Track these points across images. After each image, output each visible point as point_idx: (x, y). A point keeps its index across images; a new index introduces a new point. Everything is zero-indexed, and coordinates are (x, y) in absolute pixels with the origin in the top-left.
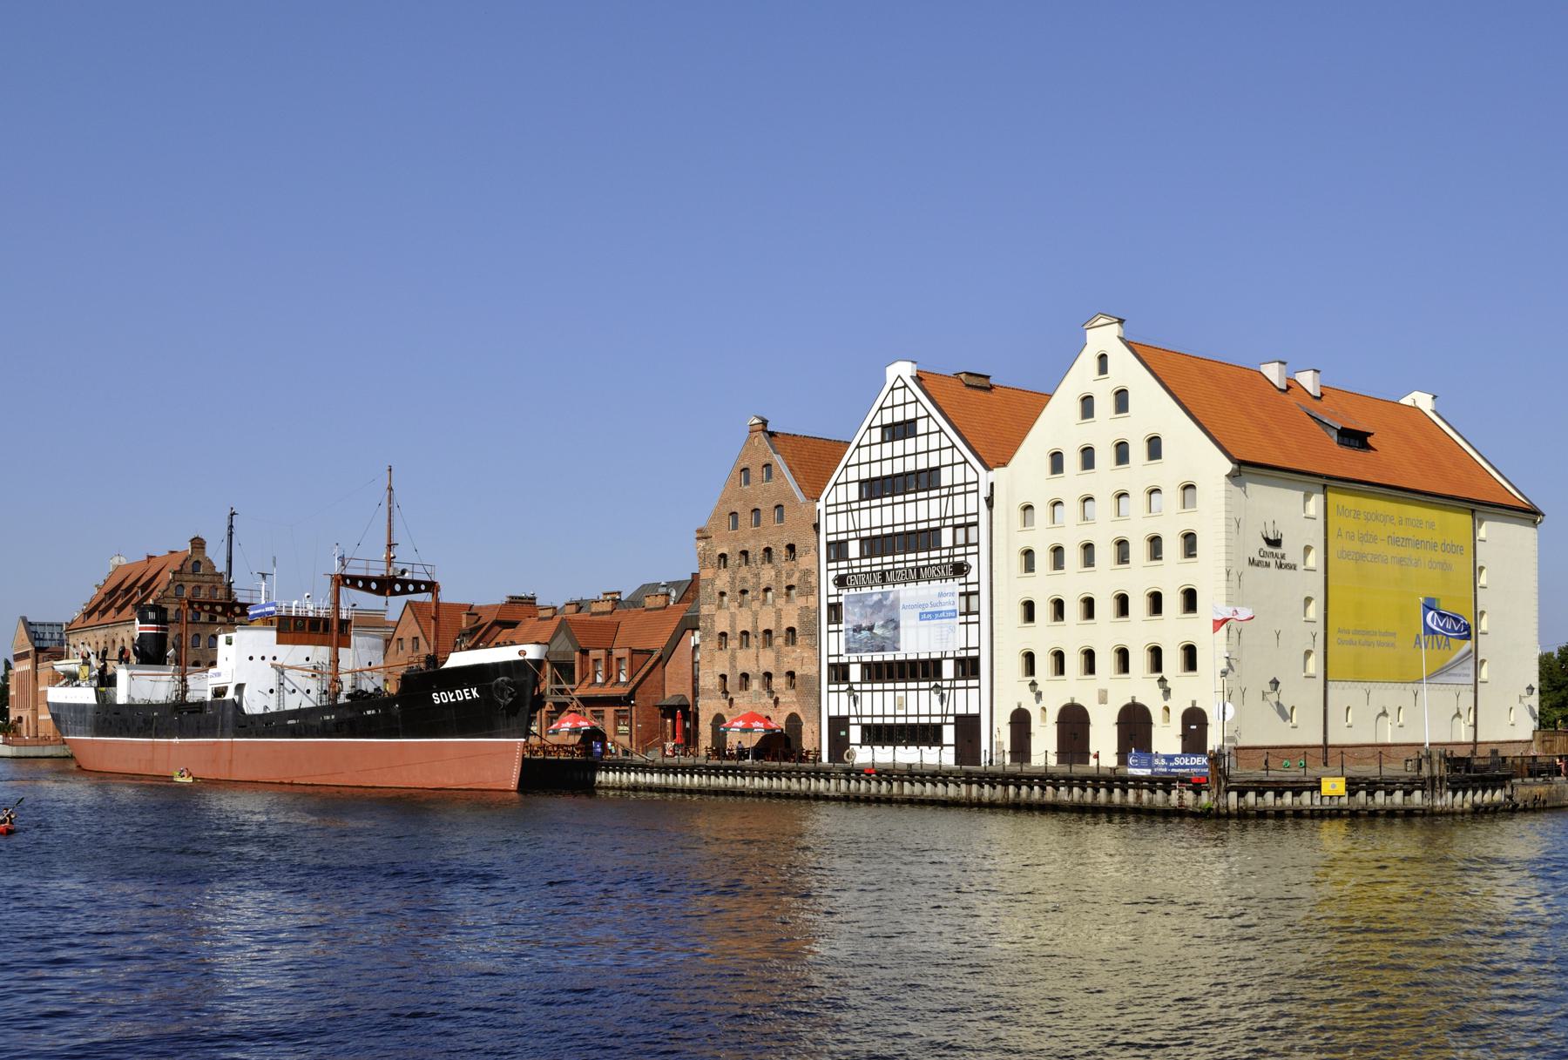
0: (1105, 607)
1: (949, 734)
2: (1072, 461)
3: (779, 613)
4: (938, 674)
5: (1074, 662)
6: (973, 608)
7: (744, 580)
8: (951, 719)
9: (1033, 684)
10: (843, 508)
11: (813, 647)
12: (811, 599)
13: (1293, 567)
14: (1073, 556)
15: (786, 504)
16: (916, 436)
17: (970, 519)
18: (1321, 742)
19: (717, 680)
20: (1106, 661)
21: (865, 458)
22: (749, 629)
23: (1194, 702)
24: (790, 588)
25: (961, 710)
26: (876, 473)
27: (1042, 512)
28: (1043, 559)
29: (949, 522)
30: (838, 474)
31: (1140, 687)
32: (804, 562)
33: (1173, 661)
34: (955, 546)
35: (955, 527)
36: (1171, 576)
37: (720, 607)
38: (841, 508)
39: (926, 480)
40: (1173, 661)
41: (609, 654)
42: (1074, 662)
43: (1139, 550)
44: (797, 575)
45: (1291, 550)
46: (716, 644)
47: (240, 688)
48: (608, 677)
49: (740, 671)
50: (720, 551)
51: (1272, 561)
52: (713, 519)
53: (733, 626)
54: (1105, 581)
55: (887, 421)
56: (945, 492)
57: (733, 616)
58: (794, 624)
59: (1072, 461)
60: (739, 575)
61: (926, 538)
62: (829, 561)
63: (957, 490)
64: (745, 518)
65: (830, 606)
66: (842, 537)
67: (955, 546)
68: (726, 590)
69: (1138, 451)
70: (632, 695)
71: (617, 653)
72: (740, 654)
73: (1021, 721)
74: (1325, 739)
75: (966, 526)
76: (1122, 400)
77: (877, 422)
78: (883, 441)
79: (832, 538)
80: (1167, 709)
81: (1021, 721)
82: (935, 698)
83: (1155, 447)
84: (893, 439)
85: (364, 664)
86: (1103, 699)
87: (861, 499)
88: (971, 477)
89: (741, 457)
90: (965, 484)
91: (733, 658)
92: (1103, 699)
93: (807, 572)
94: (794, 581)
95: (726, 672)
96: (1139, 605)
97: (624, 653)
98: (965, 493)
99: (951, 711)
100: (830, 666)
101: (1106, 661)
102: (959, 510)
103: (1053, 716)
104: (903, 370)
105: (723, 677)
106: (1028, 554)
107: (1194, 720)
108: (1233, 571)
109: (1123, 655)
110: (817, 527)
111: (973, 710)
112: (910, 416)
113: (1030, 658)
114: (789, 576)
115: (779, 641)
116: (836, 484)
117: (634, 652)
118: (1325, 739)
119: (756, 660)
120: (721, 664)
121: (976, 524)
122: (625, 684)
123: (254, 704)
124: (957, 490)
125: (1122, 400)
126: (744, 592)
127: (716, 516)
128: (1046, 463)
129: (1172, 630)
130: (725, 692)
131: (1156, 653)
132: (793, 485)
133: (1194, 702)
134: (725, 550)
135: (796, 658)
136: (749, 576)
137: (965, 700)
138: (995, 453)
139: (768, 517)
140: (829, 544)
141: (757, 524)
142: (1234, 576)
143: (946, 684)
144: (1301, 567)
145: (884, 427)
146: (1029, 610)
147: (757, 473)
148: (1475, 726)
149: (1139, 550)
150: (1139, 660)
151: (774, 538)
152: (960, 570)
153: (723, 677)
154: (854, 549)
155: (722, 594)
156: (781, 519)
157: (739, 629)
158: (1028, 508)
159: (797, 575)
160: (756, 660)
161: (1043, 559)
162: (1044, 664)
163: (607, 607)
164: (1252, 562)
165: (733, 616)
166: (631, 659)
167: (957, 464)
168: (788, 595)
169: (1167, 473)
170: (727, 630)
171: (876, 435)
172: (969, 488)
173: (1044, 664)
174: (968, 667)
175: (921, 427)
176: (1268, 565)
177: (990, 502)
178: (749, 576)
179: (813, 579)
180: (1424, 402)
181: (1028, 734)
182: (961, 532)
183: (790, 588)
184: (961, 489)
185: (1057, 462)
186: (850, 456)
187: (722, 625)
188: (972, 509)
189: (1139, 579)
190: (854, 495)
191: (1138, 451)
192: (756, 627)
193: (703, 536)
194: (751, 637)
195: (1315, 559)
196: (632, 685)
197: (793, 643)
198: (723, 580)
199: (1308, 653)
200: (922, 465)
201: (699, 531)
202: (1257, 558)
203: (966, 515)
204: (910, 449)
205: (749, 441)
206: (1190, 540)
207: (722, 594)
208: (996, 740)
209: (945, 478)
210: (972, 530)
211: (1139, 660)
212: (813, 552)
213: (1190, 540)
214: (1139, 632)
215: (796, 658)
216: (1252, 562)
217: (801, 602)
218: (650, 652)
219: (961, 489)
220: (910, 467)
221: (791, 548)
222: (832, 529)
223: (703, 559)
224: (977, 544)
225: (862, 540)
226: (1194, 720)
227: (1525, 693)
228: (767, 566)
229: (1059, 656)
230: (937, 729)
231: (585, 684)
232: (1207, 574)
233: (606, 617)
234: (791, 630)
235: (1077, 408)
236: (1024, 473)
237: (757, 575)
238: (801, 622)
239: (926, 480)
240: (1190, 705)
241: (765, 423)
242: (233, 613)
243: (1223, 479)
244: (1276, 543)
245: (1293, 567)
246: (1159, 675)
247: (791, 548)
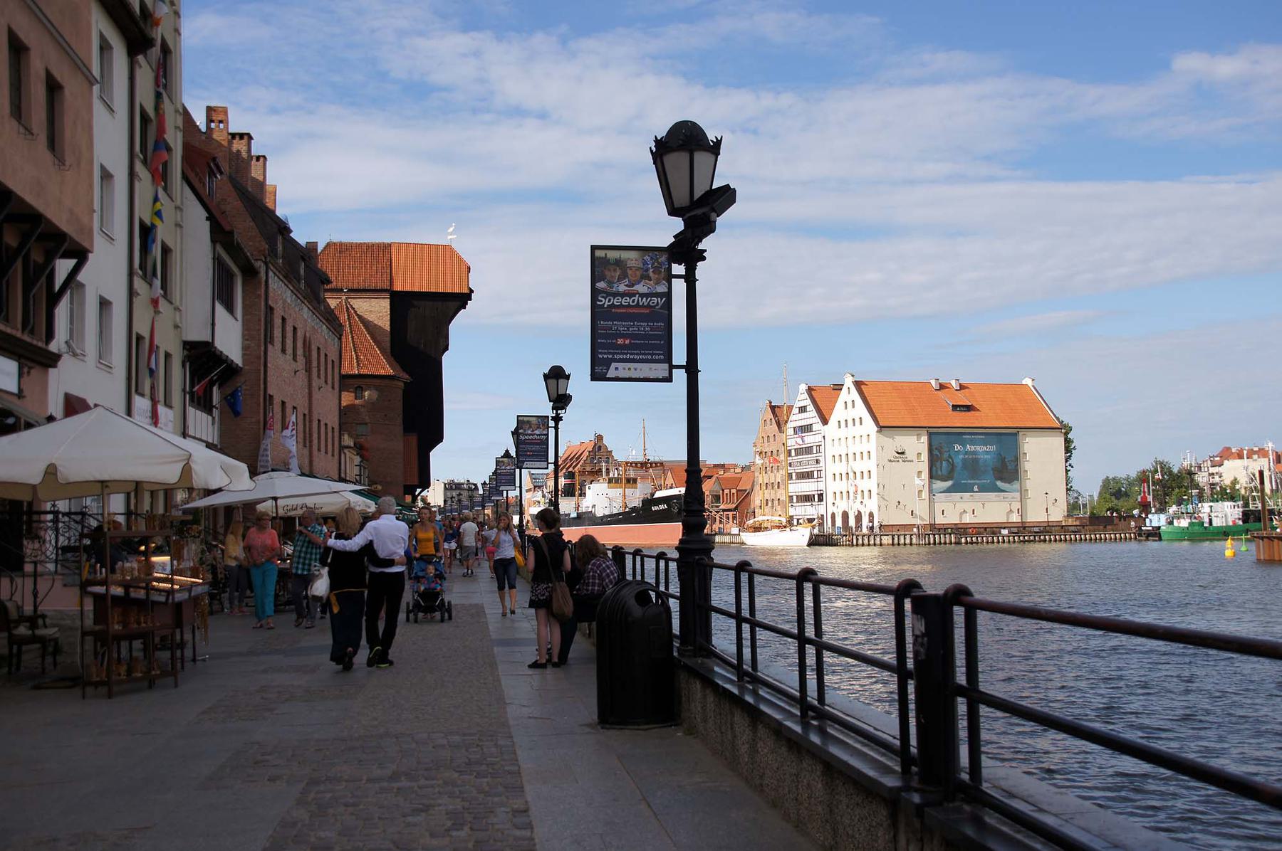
2: (843, 424)
30: (790, 425)
39: (807, 429)
45: (909, 455)
47: (594, 506)
59: (843, 424)
61: (808, 450)
85: (635, 497)
104: (803, 387)
107: (871, 515)
119: (768, 494)
123: (600, 512)
135: (781, 494)
138: (825, 421)
152: (818, 462)
160: (768, 494)
167: (818, 426)
174: (821, 499)
180: (1027, 381)
186: (792, 417)
215: (781, 494)
226: (871, 515)
239: (807, 429)
242: (595, 474)
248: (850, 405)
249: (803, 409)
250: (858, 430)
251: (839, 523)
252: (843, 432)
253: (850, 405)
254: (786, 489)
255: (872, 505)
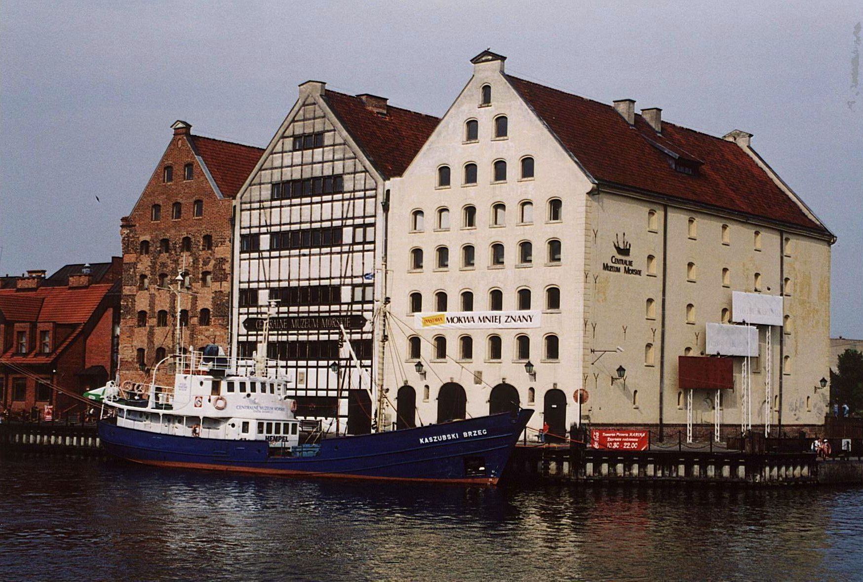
0: (482, 301)
1: (344, 407)
2: (458, 175)
3: (195, 299)
4: (336, 355)
5: (454, 347)
6: (369, 297)
7: (164, 265)
8: (345, 394)
9: (419, 365)
10: (256, 205)
11: (225, 327)
12: (225, 284)
13: (638, 272)
14: (456, 256)
15: (205, 200)
16: (323, 147)
17: (368, 220)
18: (658, 422)
19: (135, 353)
20: (481, 347)
21: (277, 163)
22: (167, 309)
23: (555, 384)
24: (206, 273)
25: (355, 386)
26: (287, 177)
27: (429, 219)
28: (430, 258)
29: (350, 222)
31: (509, 370)
32: (220, 251)
33: (538, 349)
34: (354, 243)
35: (355, 227)
36: (539, 276)
37: (141, 288)
38: (256, 205)
39: (330, 185)
40: (538, 349)
41: (34, 326)
42: (454, 347)
43: (512, 254)
44: (213, 262)
45: (637, 257)
46: (135, 321)
48: (31, 348)
49: (157, 343)
50: (142, 238)
51: (622, 267)
52: (135, 209)
53: (152, 305)
54: (482, 278)
55: (299, 131)
56: (347, 196)
57: (152, 297)
58: (209, 305)
59: (458, 175)
60: (159, 261)
61: (327, 237)
62: (241, 253)
63: (358, 194)
64: (167, 210)
65: (242, 291)
66: (255, 231)
67: (354, 243)
68: (148, 273)
69: (514, 169)
70: (54, 364)
71: (41, 326)
72: (158, 331)
73: (407, 396)
74: (661, 419)
75: (365, 226)
76: (501, 126)
77: (289, 132)
78: (295, 150)
79: (245, 232)
80: (532, 389)
81: (407, 396)
82: (333, 375)
83: (528, 167)
84: (303, 148)
86: (478, 379)
87: (272, 199)
88: (370, 183)
89: (166, 156)
90: (365, 190)
91: (151, 334)
92: (478, 379)
93: (223, 261)
94: (210, 267)
95: (145, 346)
96: (510, 300)
97: (48, 326)
98: (365, 198)
99: (346, 386)
100: (239, 342)
101: (481, 347)
102: (359, 212)
103: (434, 393)
105: (141, 351)
106: (418, 253)
107: (555, 398)
108: (590, 275)
109: (496, 343)
110: (232, 220)
111: (365, 386)
112: (319, 128)
113: (415, 342)
114: (206, 263)
115: (195, 320)
116: (250, 185)
117: (57, 325)
118: (661, 419)
120: (140, 339)
121: (373, 225)
122: (48, 355)
124: (358, 194)
125: (501, 126)
126: (163, 276)
127: (139, 207)
128: (435, 177)
129: (538, 323)
130: (143, 364)
131: (524, 342)
132: (212, 184)
133: (555, 384)
134: (147, 238)
136: (169, 262)
137: (358, 377)
139: (188, 212)
140: (241, 235)
141: (178, 216)
142: (591, 279)
143: (343, 363)
144: (644, 273)
145: (296, 137)
146: (416, 301)
147: (179, 170)
148: (779, 412)
149: (512, 254)
150: (509, 347)
151: (194, 229)
153: (141, 351)
154: (265, 242)
155: (143, 277)
156: (200, 213)
157: (157, 309)
158: (418, 213)
159: (213, 262)
161: (430, 258)
162: (428, 349)
163: (32, 284)
164: (606, 267)
165: (152, 297)
166: (55, 333)
168: (204, 280)
169: (539, 190)
170: (147, 309)
171: (289, 143)
172: (368, 193)
173: (428, 349)
174: (364, 349)
175: (328, 139)
176: (618, 270)
177: (386, 208)
178: (169, 262)
179: (227, 267)
181: (412, 408)
182: (360, 231)
183: (206, 273)
184: (361, 194)
185: (444, 175)
187: (142, 303)
188: (370, 210)
189: (510, 277)
190: (266, 192)
191: (514, 169)
192: (173, 307)
193: (127, 223)
194: (169, 318)
195: (656, 267)
196: (54, 356)
197: (208, 324)
198: (144, 264)
199: (649, 346)
200: (328, 172)
201: (123, 220)
202: (610, 264)
203: (364, 217)
204: (318, 157)
205: (173, 143)
206: (555, 247)
207: (143, 277)
208: (386, 414)
209: (348, 185)
210: (370, 230)
211: (509, 347)
212: (227, 242)
213: (555, 247)
214: (509, 323)
216: (606, 267)
217: (216, 286)
218: (74, 326)
219: (361, 194)
220: (318, 173)
221: (208, 239)
222: (246, 223)
223: (127, 245)
224: (374, 242)
225: (273, 234)
226: (555, 398)
227: (819, 385)
228: (189, 253)
229: (441, 343)
230: (334, 401)
231: (9, 354)
232: (569, 276)
233: (30, 294)
234: (205, 311)
235: (463, 130)
236: (415, 184)
237: (176, 262)
238: (214, 304)
239: (330, 185)
240: (552, 387)
241: (188, 126)
243: (585, 196)
244: (625, 252)
245: (638, 272)
246: (526, 361)
247: (208, 239)
248: (487, 128)
249: (309, 141)
250: (514, 188)
251: (427, 413)
252: (458, 194)
253: (487, 128)
254: (227, 323)
255: (567, 375)
